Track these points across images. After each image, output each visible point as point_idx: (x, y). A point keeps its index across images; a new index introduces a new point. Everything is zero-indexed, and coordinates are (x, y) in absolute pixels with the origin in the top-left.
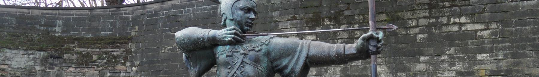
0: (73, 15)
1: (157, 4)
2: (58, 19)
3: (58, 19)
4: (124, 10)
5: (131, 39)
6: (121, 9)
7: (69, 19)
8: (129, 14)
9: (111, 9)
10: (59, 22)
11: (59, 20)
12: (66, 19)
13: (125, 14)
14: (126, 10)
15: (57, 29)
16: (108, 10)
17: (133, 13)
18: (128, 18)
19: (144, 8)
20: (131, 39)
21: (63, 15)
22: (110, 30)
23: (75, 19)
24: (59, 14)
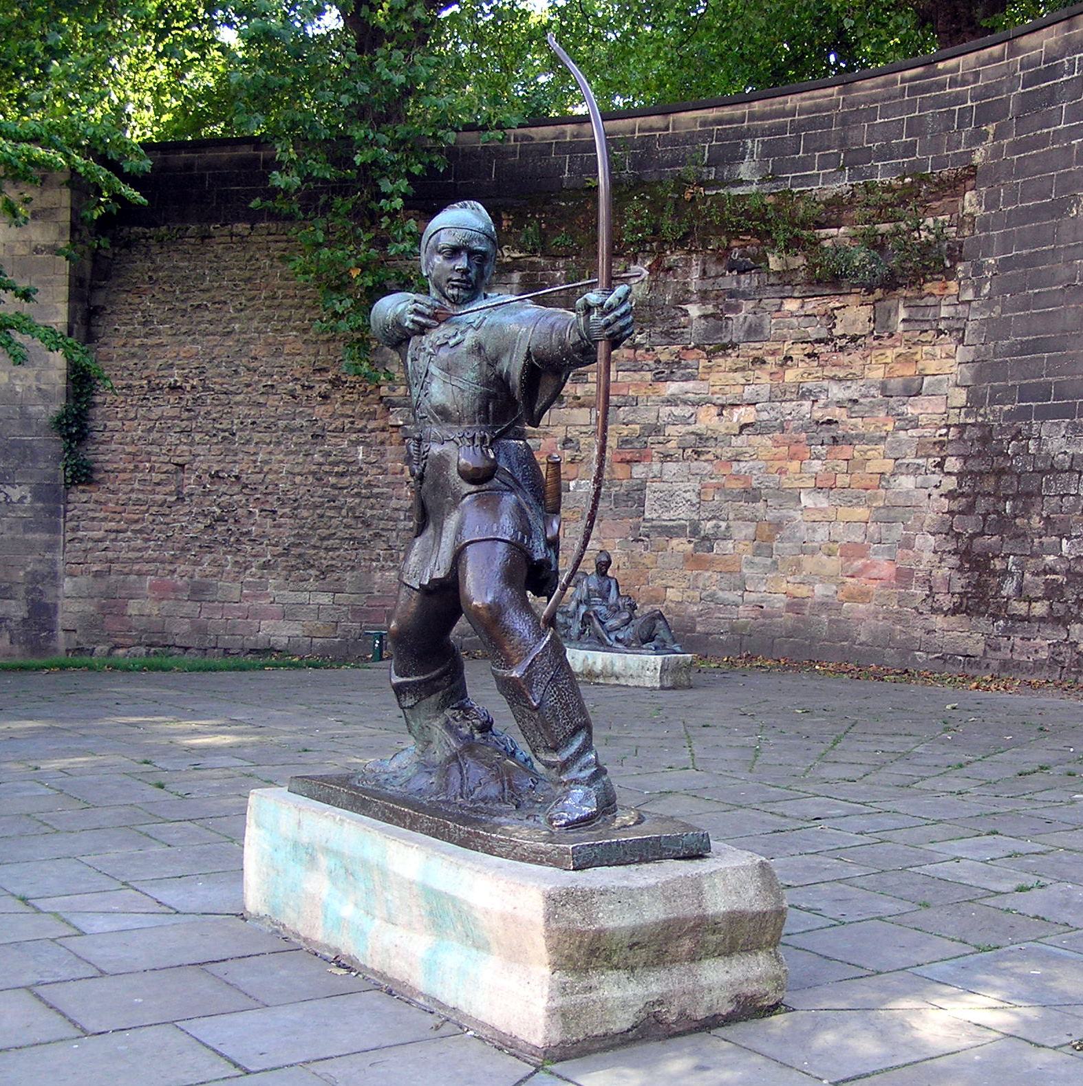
0: (792, 113)
1: (1054, 28)
2: (751, 134)
3: (751, 134)
4: (946, 71)
5: (971, 174)
6: (940, 66)
7: (782, 129)
8: (964, 83)
9: (908, 74)
10: (754, 145)
11: (753, 137)
12: (771, 131)
13: (953, 83)
14: (956, 69)
15: (745, 170)
16: (899, 76)
17: (977, 74)
18: (959, 99)
19: (1014, 52)
20: (971, 174)
21: (763, 116)
22: (909, 150)
23: (797, 128)
24: (752, 116)
